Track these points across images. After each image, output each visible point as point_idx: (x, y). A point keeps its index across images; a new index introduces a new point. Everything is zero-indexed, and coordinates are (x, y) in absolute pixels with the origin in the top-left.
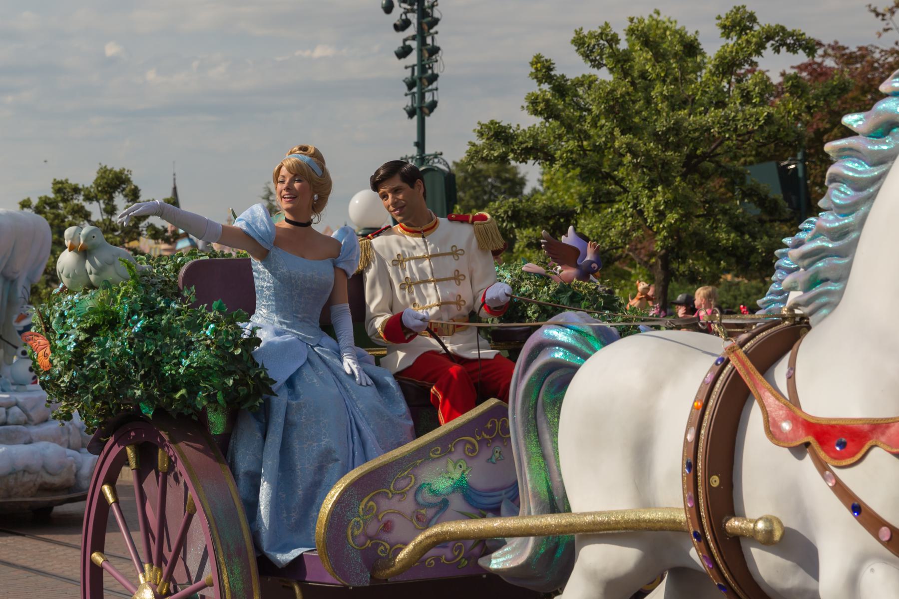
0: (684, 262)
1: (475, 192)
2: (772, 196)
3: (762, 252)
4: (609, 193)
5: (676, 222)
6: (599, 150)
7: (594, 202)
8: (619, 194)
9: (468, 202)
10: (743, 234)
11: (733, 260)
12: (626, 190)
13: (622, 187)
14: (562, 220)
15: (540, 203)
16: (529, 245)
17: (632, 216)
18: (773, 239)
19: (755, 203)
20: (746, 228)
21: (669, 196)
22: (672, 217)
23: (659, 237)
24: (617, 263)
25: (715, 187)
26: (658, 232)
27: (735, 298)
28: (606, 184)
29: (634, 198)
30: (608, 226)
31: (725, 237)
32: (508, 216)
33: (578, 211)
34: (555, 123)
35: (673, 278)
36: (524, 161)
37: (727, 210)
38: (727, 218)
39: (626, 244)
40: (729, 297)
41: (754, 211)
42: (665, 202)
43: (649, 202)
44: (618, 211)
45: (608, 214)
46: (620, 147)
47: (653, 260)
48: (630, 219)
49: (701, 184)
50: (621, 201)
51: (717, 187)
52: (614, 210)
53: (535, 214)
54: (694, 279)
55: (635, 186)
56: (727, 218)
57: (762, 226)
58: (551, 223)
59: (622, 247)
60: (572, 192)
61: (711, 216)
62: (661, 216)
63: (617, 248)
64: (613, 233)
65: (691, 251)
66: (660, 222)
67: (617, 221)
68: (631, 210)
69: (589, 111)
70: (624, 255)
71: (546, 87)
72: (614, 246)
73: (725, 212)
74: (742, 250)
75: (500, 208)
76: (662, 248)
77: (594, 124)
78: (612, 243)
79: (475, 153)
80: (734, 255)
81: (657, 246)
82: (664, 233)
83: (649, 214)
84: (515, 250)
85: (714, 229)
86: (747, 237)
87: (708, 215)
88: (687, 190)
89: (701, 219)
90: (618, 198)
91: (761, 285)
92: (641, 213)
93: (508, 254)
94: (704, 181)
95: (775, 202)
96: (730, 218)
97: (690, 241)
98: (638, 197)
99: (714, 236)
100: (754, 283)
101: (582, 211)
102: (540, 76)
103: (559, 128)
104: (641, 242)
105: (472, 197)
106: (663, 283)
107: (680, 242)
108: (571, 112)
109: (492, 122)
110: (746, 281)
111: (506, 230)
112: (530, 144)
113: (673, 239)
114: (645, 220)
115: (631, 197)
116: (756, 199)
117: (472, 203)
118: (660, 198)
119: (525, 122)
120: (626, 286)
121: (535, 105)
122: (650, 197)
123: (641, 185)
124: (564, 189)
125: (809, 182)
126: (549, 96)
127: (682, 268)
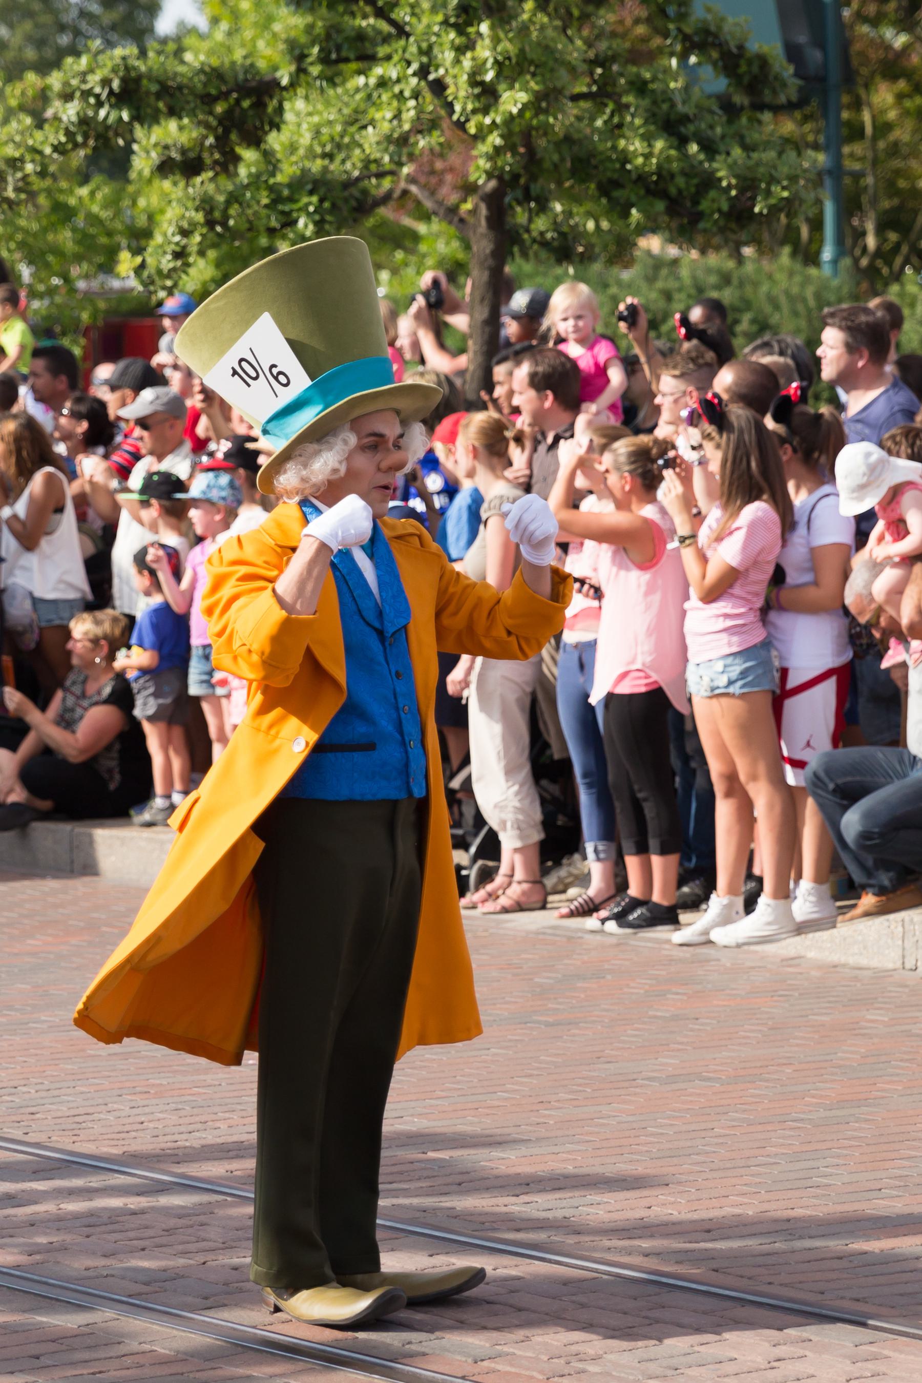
0: (543, 207)
1: (37, 26)
2: (754, 46)
3: (730, 186)
4: (361, 36)
5: (521, 111)
7: (324, 59)
8: (387, 39)
9: (20, 49)
10: (683, 142)
11: (660, 206)
12: (402, 31)
13: (393, 23)
14: (246, 104)
16: (165, 168)
17: (416, 95)
18: (755, 155)
19: (715, 64)
20: (691, 128)
21: (506, 46)
22: (513, 100)
23: (484, 148)
24: (384, 212)
25: (621, 22)
26: (479, 137)
27: (668, 296)
28: (353, 15)
29: (421, 52)
30: (357, 120)
31: (643, 149)
32: (111, 92)
33: (285, 82)
35: (516, 249)
37: (645, 83)
38: (646, 102)
39: (400, 164)
40: (654, 295)
41: (714, 82)
42: (496, 62)
43: (457, 61)
44: (383, 83)
45: (358, 90)
47: (468, 206)
48: (412, 103)
49: (585, 17)
50: (388, 58)
51: (629, 22)
52: (372, 81)
53: (180, 88)
54: (564, 250)
55: (425, 20)
56: (646, 102)
57: (730, 122)
58: (219, 109)
59: (392, 173)
61: (609, 96)
62: (487, 95)
63: (380, 175)
65: (559, 183)
66: (485, 111)
67: (378, 106)
68: (414, 81)
70: (397, 194)
73: (640, 87)
74: (681, 181)
75: (91, 71)
76: (489, 175)
78: (367, 162)
80: (663, 194)
81: (479, 169)
82: (495, 139)
83: (460, 91)
84: (133, 175)
85: (616, 129)
86: (694, 148)
87: (603, 94)
88: (550, 33)
89: (584, 104)
90: (382, 51)
91: (731, 264)
92: (439, 87)
93: (115, 185)
94: (590, 9)
95: (763, 61)
96: (655, 103)
97: (556, 157)
98: (430, 47)
99: (614, 148)
100: (713, 259)
101: (293, 85)
104: (441, 156)
105: (29, 39)
106: (490, 262)
107: (532, 159)
110: (694, 254)
111: (108, 128)
113: (514, 153)
114: (450, 107)
115: (413, 49)
116: (715, 55)
117: (30, 54)
118: (484, 51)
120: (406, 265)
122: (461, 50)
123: (440, 18)
124: (256, 24)
125: (846, 13)
127: (541, 224)
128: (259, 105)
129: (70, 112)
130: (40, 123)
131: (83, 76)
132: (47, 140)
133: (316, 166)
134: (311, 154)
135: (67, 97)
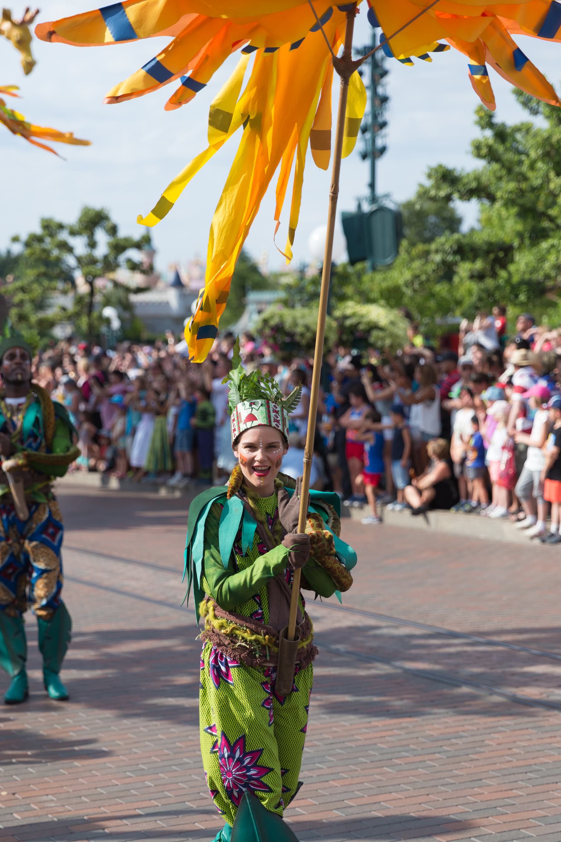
6: (533, 189)
7: (530, 237)
8: (553, 230)
15: (481, 238)
30: (542, 259)
34: (496, 166)
36: (469, 200)
44: (553, 246)
46: (555, 188)
60: (510, 227)
64: (547, 266)
69: (528, 155)
71: (489, 133)
72: (547, 277)
77: (532, 167)
79: (423, 194)
90: (551, 234)
102: (483, 122)
103: (500, 170)
108: (509, 156)
109: (440, 166)
112: (474, 185)
119: (469, 165)
121: (478, 149)
126: (491, 141)
128: (506, 255)
129: (438, 258)
130: (427, 261)
131: (443, 245)
132: (430, 268)
133: (527, 277)
134: (524, 273)
135: (437, 251)
